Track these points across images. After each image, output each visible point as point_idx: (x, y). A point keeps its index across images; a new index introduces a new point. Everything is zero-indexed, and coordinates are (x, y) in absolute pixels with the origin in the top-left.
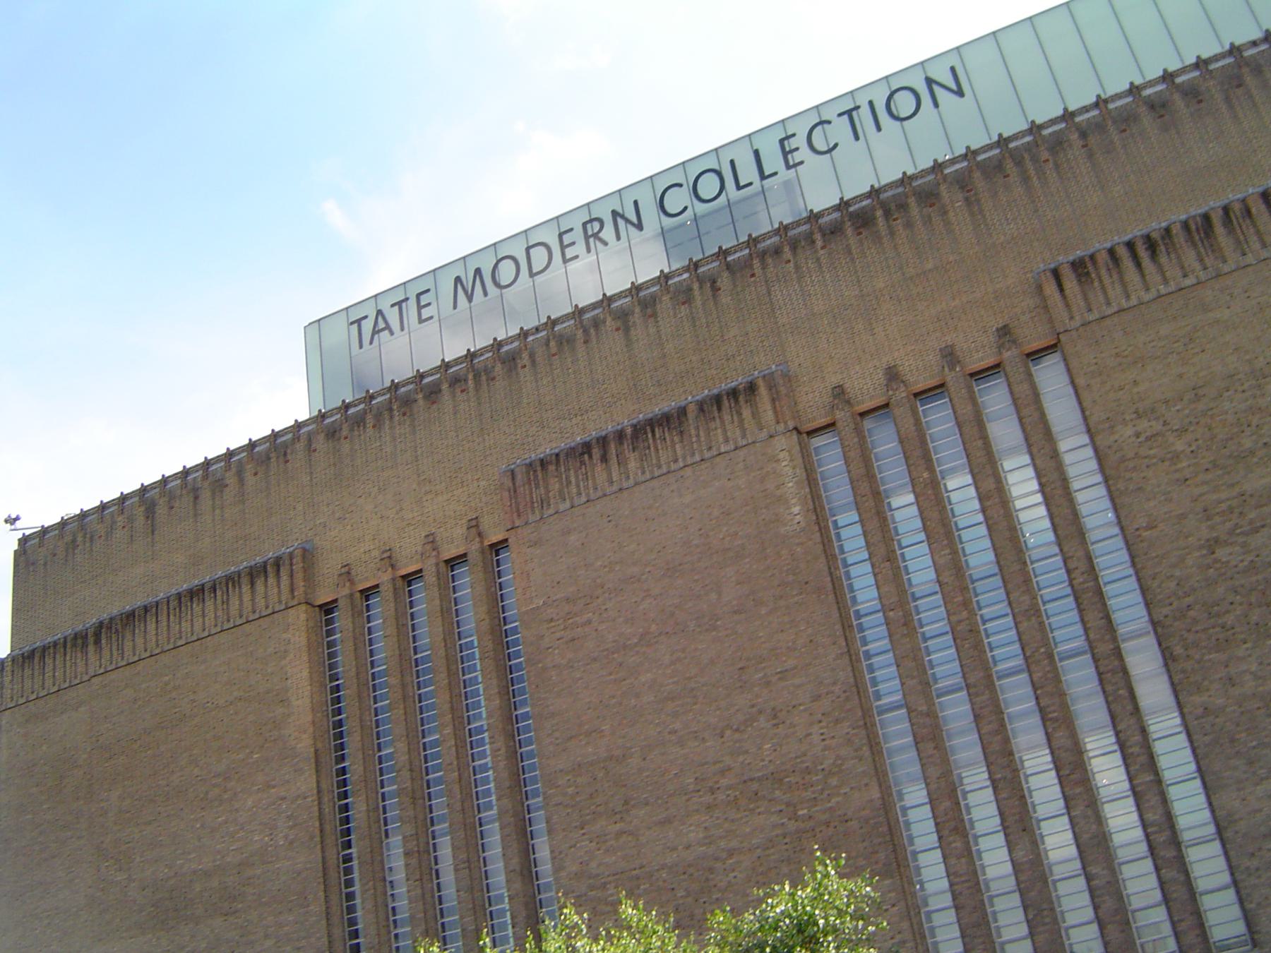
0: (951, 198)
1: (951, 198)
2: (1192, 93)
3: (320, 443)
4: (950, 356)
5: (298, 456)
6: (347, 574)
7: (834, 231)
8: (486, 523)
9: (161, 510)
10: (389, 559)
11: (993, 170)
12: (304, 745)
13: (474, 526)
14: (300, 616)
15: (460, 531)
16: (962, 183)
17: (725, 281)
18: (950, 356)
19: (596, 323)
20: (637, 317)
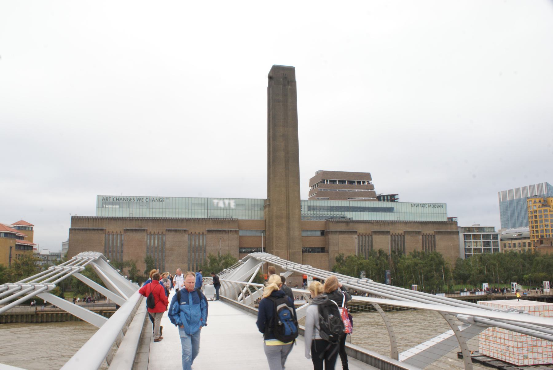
0: (162, 221)
1: (162, 221)
2: (179, 220)
3: (107, 219)
4: (158, 233)
5: (105, 220)
6: (109, 232)
7: (153, 220)
8: (122, 232)
9: (90, 220)
10: (113, 232)
11: (165, 220)
12: (104, 245)
13: (121, 232)
14: (104, 235)
15: (119, 232)
16: (163, 220)
17: (144, 220)
18: (158, 233)
19: (134, 219)
20: (137, 221)
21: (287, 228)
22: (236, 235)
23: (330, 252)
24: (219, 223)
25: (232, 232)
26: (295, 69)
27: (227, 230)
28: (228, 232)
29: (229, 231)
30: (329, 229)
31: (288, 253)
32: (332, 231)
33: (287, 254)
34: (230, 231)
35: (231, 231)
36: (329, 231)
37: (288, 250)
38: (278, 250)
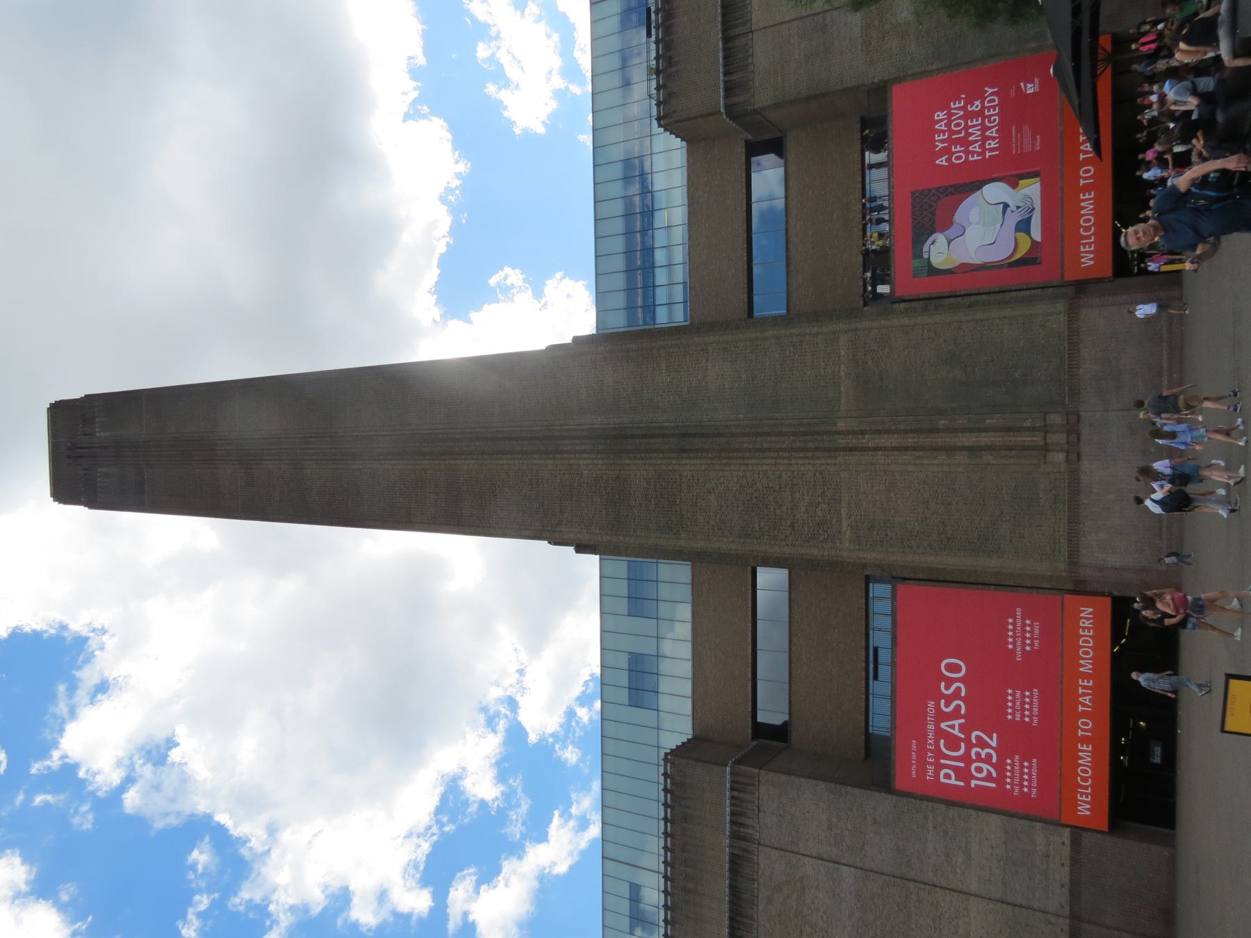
21: (683, 450)
22: (763, 789)
23: (876, 74)
24: (690, 885)
25: (742, 814)
26: (75, 392)
27: (731, 846)
28: (744, 844)
29: (735, 836)
30: (720, 112)
31: (865, 440)
32: (729, 90)
33: (876, 449)
34: (733, 823)
35: (737, 819)
36: (727, 106)
37: (842, 441)
38: (845, 524)
